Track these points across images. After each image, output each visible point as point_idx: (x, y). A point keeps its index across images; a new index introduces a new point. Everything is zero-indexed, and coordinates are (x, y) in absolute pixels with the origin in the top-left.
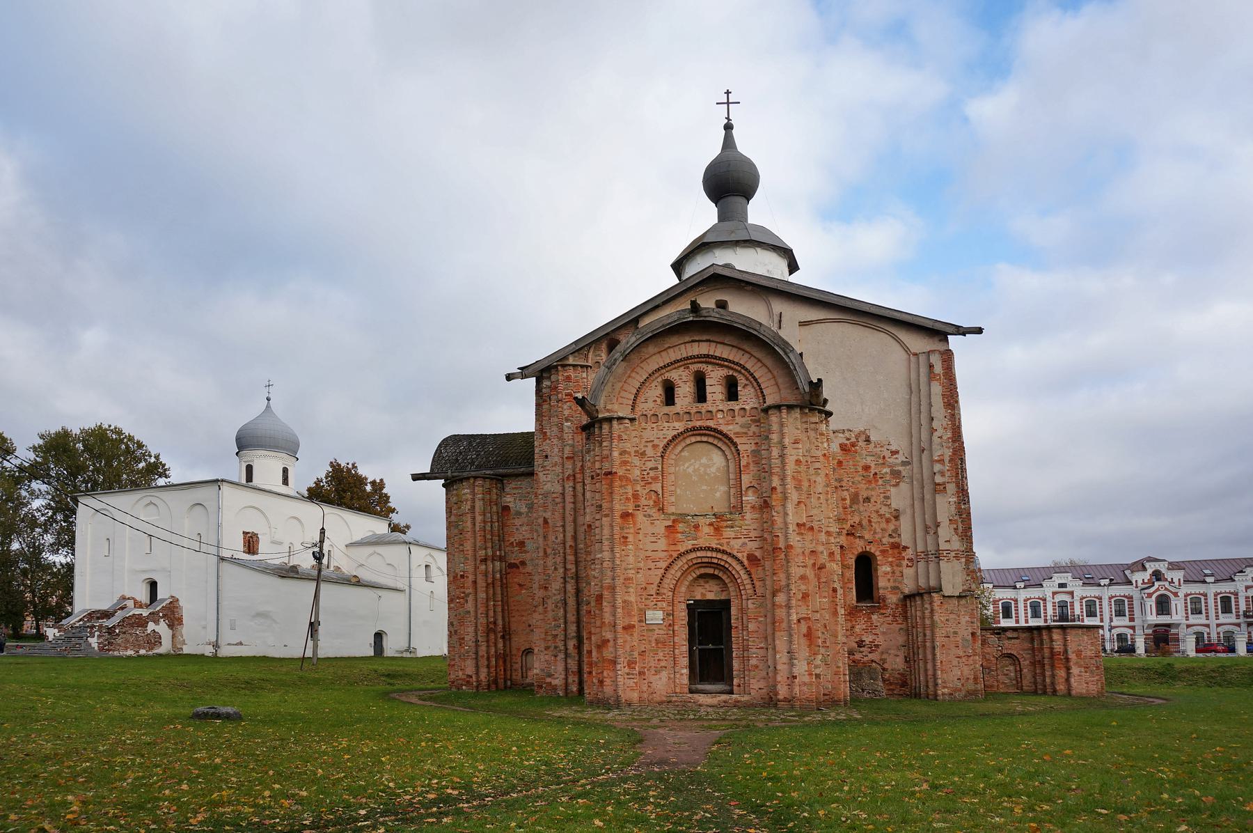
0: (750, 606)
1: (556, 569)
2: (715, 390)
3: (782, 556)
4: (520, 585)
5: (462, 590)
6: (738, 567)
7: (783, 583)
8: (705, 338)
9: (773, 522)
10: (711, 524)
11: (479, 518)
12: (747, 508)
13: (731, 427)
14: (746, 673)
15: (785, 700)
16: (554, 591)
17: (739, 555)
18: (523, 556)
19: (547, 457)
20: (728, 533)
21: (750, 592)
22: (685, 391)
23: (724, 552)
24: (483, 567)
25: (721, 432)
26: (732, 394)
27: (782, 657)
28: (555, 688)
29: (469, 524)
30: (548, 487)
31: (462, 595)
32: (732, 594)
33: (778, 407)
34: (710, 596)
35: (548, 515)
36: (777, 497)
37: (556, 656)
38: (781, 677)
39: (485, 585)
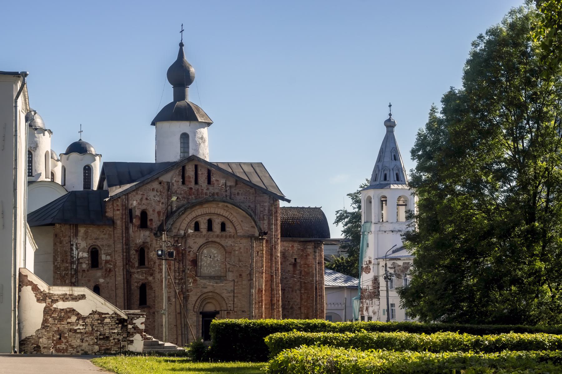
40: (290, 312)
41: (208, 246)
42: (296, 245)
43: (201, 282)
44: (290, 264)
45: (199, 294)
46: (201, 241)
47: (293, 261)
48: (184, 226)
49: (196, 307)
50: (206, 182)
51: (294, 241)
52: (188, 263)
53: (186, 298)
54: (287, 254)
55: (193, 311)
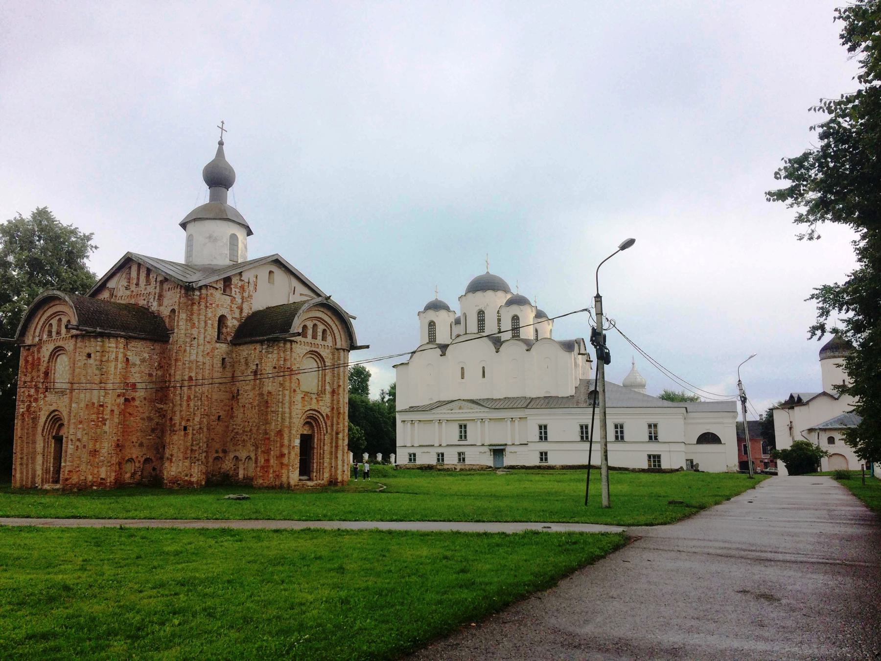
0: (326, 438)
1: (198, 409)
2: (320, 334)
3: (342, 417)
4: (130, 414)
5: (101, 416)
6: (322, 420)
7: (342, 429)
8: (322, 310)
9: (338, 402)
10: (316, 398)
11: (120, 366)
12: (327, 393)
13: (324, 353)
14: (321, 470)
15: (340, 482)
16: (195, 422)
17: (324, 415)
18: (134, 394)
19: (195, 338)
20: (321, 403)
21: (325, 431)
22: (310, 332)
23: (319, 412)
24: (118, 401)
25: (320, 355)
26: (324, 338)
27: (340, 463)
28: (191, 483)
29: (113, 369)
30: (193, 357)
31: (101, 419)
32: (316, 432)
33: (344, 350)
34: (305, 432)
35: (193, 375)
36: (341, 389)
37: (195, 463)
38: (339, 472)
39: (118, 413)
40: (249, 436)
41: (59, 353)
42: (258, 346)
43: (50, 397)
44: (251, 372)
45: (47, 413)
46: (51, 347)
47: (254, 367)
48: (38, 330)
49: (45, 430)
50: (145, 281)
51: (257, 342)
52: (42, 375)
53: (35, 420)
54: (249, 358)
55: (42, 435)
